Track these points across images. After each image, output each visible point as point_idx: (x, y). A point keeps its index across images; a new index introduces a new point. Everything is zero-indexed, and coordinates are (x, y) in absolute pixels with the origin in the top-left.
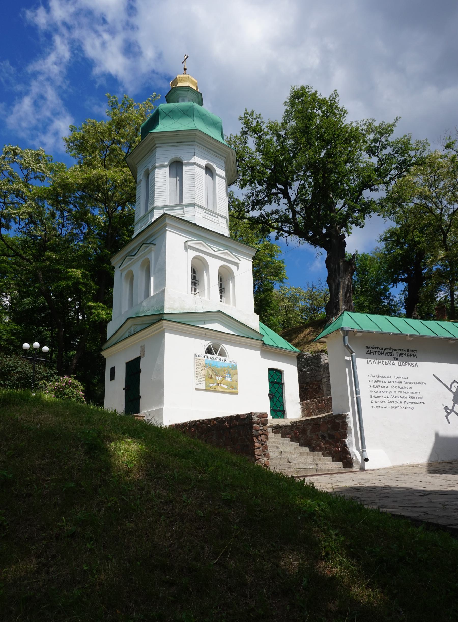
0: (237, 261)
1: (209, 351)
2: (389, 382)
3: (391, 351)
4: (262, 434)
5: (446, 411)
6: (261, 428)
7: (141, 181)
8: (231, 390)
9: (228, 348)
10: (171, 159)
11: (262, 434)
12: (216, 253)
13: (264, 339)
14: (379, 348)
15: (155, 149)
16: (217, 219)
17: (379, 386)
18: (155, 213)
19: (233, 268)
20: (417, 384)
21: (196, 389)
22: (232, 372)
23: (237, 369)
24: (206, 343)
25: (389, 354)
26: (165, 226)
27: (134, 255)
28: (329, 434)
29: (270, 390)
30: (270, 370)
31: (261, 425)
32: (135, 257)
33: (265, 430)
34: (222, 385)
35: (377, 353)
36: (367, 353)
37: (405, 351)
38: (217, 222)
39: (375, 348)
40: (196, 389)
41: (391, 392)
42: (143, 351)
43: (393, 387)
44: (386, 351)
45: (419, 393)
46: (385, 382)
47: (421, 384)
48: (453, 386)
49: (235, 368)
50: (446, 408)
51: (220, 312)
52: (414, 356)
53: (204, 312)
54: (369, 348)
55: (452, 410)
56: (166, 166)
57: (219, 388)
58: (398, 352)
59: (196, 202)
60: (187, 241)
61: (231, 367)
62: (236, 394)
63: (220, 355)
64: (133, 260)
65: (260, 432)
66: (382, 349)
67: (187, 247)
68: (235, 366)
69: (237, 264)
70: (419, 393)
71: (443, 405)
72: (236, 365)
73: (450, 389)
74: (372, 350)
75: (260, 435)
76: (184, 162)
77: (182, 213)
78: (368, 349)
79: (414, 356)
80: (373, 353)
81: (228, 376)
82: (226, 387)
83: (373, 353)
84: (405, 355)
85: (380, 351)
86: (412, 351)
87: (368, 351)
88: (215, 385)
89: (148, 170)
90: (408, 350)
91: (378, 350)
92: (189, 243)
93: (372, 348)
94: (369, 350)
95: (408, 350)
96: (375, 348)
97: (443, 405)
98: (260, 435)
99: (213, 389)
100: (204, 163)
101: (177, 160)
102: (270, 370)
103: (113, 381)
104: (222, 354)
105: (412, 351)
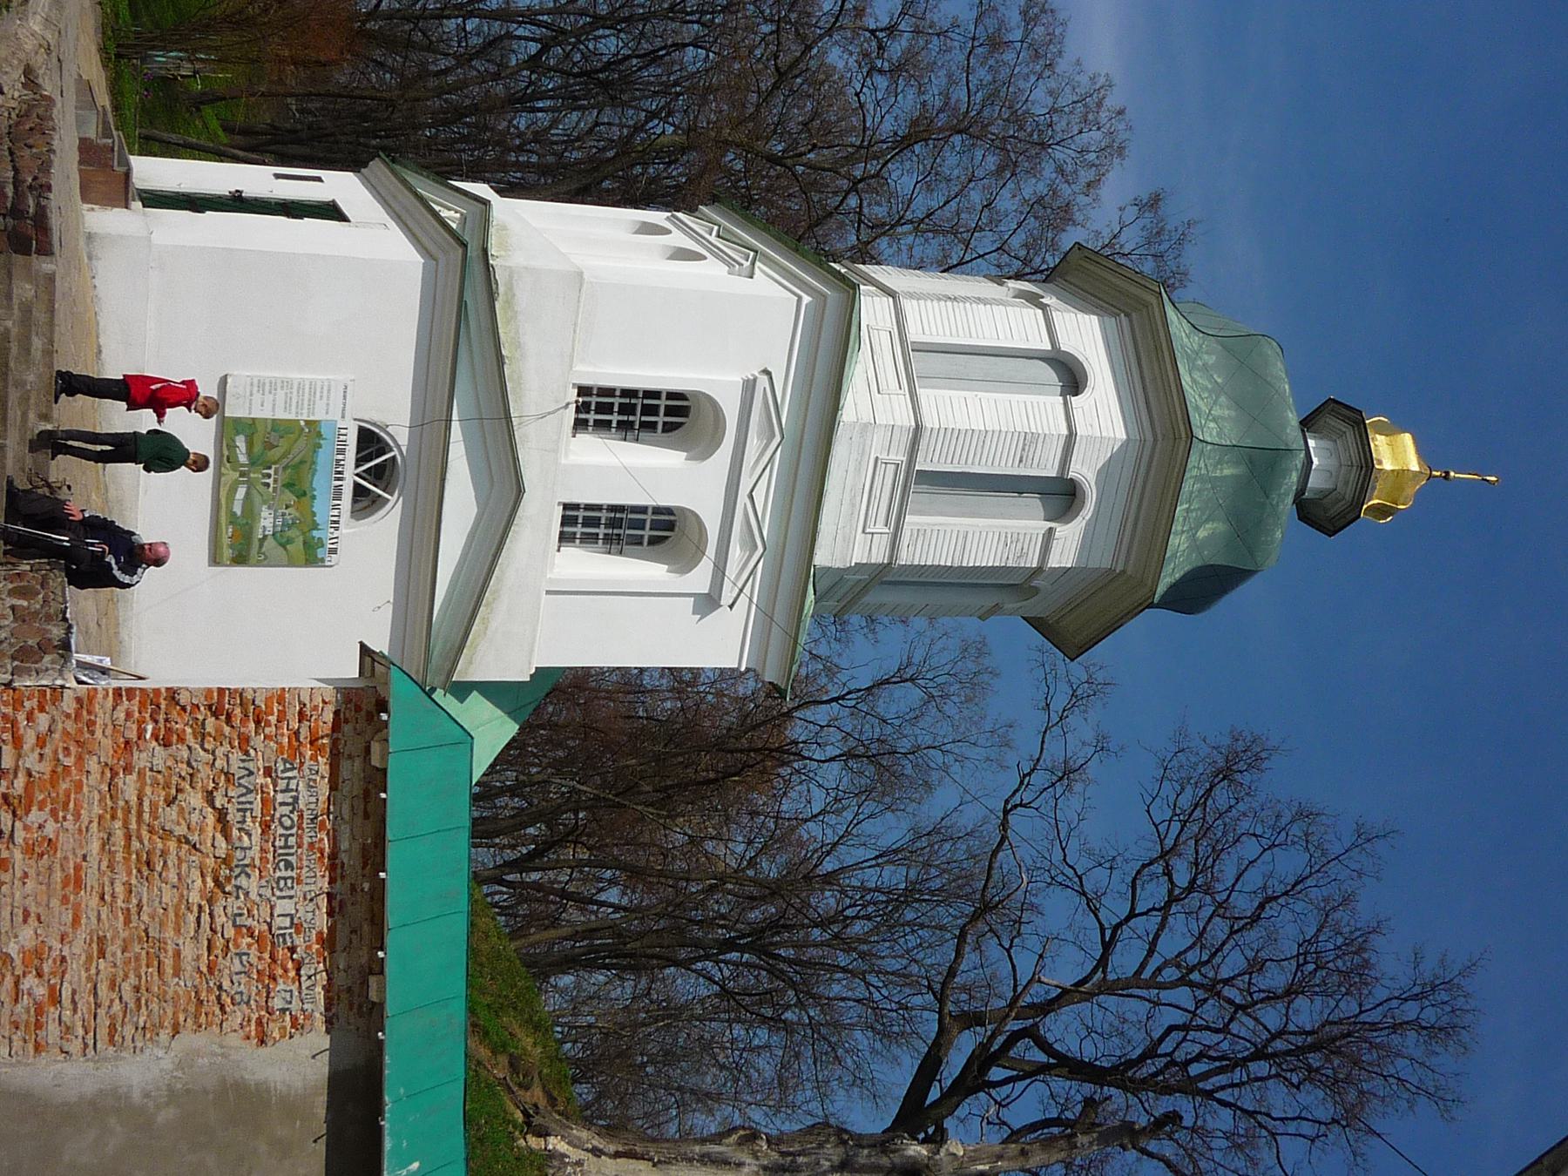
1: (370, 442)
9: (388, 522)
10: (1081, 358)
12: (742, 498)
15: (1116, 315)
19: (699, 578)
24: (399, 431)
32: (713, 239)
34: (241, 492)
42: (366, 224)
49: (311, 554)
51: (520, 491)
53: (508, 418)
60: (767, 372)
62: (215, 560)
63: (359, 491)
68: (320, 553)
76: (1075, 401)
82: (238, 509)
88: (243, 459)
99: (226, 453)
104: (365, 502)
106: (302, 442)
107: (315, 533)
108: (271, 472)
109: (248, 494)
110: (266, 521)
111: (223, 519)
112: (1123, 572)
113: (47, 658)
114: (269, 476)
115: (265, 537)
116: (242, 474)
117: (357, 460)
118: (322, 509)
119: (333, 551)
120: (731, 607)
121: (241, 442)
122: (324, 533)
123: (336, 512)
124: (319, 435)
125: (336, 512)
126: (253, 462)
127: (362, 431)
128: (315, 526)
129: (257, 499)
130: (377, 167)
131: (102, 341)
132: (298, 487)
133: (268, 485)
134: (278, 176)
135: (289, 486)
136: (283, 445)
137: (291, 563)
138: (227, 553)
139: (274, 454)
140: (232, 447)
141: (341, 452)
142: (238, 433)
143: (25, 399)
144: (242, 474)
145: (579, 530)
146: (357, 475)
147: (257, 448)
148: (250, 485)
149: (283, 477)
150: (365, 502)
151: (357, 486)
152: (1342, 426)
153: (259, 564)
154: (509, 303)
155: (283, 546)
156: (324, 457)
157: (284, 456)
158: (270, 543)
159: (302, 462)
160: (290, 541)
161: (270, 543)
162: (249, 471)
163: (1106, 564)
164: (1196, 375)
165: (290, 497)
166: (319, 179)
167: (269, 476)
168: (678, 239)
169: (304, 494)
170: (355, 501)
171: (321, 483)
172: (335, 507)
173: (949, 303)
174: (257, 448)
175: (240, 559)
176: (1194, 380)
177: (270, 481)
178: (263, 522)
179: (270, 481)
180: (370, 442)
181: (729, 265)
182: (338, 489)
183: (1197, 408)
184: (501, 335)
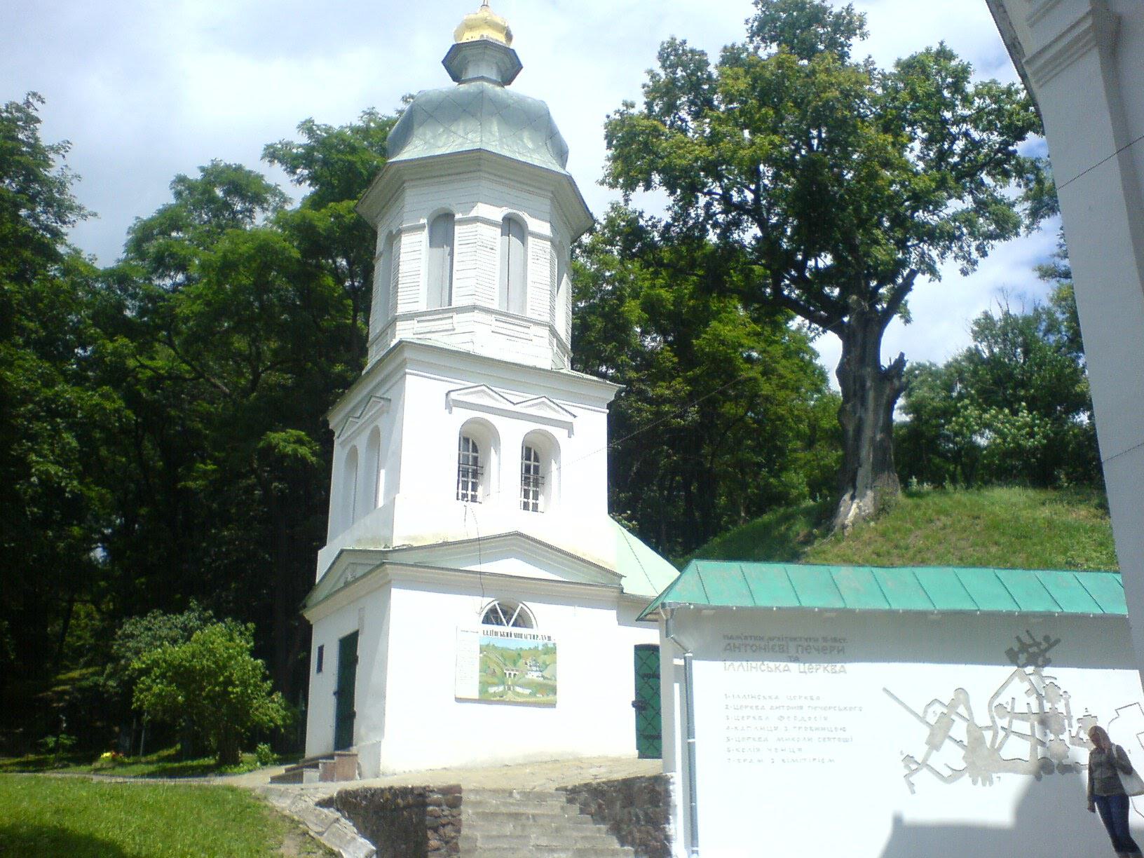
0: (569, 418)
1: (491, 617)
2: (772, 708)
3: (784, 643)
4: (448, 824)
5: (907, 766)
6: (446, 813)
7: (381, 254)
8: (540, 697)
9: (537, 609)
11: (448, 824)
12: (517, 408)
13: (623, 582)
14: (756, 638)
15: (404, 190)
16: (526, 330)
17: (748, 717)
18: (398, 328)
19: (559, 434)
20: (840, 710)
21: (458, 700)
22: (543, 657)
23: (555, 653)
24: (485, 603)
25: (777, 649)
26: (403, 364)
27: (359, 418)
28: (646, 814)
29: (637, 694)
30: (639, 649)
31: (444, 807)
32: (361, 421)
33: (453, 816)
34: (518, 689)
35: (748, 647)
36: (725, 649)
37: (816, 640)
38: (527, 336)
39: (746, 638)
40: (458, 700)
41: (776, 728)
42: (361, 620)
43: (781, 718)
44: (771, 643)
45: (844, 729)
46: (763, 708)
47: (851, 709)
48: (931, 710)
49: (551, 651)
50: (909, 759)
52: (838, 652)
53: (479, 539)
54: (731, 638)
55: (924, 764)
56: (422, 227)
57: (510, 696)
58: (799, 643)
59: (478, 303)
60: (449, 392)
61: (540, 648)
62: (552, 705)
64: (357, 425)
65: (444, 821)
66: (762, 639)
67: (451, 404)
68: (550, 645)
69: (569, 427)
70: (844, 729)
71: (902, 753)
72: (554, 644)
73: (923, 720)
74: (737, 642)
75: (444, 825)
77: (450, 327)
78: (728, 641)
79: (838, 652)
80: (739, 648)
81: (534, 668)
82: (527, 691)
83: (739, 648)
84: (818, 650)
85: (757, 643)
86: (835, 640)
87: (729, 644)
88: (501, 688)
89: (391, 232)
90: (825, 639)
91: (751, 642)
92: (453, 396)
93: (738, 637)
94: (731, 642)
95: (825, 639)
96: (746, 638)
97: (902, 753)
98: (444, 825)
100: (497, 214)
101: (447, 212)
102: (639, 649)
103: (321, 674)
104: (523, 621)
105: (835, 640)
106: (491, 656)
107: (540, 648)
108: (507, 673)
109: (520, 686)
110: (534, 676)
111: (532, 699)
112: (552, 192)
113: (657, 788)
114: (510, 674)
115: (543, 676)
116: (509, 689)
117: (498, 624)
118: (526, 644)
119: (549, 638)
120: (575, 416)
121: (492, 690)
122: (540, 643)
123: (529, 637)
124: (488, 645)
125: (529, 637)
126: (503, 683)
127: (487, 620)
128: (536, 648)
129: (523, 680)
130: (309, 615)
131: (440, 768)
132: (515, 658)
133: (515, 674)
134: (320, 669)
135: (515, 663)
136: (493, 666)
137: (555, 662)
138: (551, 698)
139: (498, 670)
140: (495, 694)
141: (496, 634)
142: (487, 691)
143: (505, 804)
144: (509, 689)
145: (531, 501)
146: (508, 623)
147: (496, 680)
148: (515, 684)
149: (510, 666)
150: (520, 621)
151: (514, 625)
152: (459, 57)
153: (556, 680)
154: (414, 539)
155: (547, 666)
156: (500, 643)
157: (498, 665)
158: (546, 674)
159: (502, 656)
160: (544, 663)
161: (546, 674)
162: (508, 685)
163: (548, 202)
164: (440, 144)
165: (521, 662)
166: (321, 649)
167: (510, 674)
168: (361, 443)
169: (519, 654)
170: (520, 626)
171: (513, 644)
172: (526, 638)
173: (400, 286)
174: (496, 680)
175: (554, 690)
176: (444, 145)
177: (513, 673)
178: (535, 677)
179: (513, 673)
180: (491, 617)
181: (383, 412)
182: (517, 635)
183: (461, 144)
184: (431, 543)
